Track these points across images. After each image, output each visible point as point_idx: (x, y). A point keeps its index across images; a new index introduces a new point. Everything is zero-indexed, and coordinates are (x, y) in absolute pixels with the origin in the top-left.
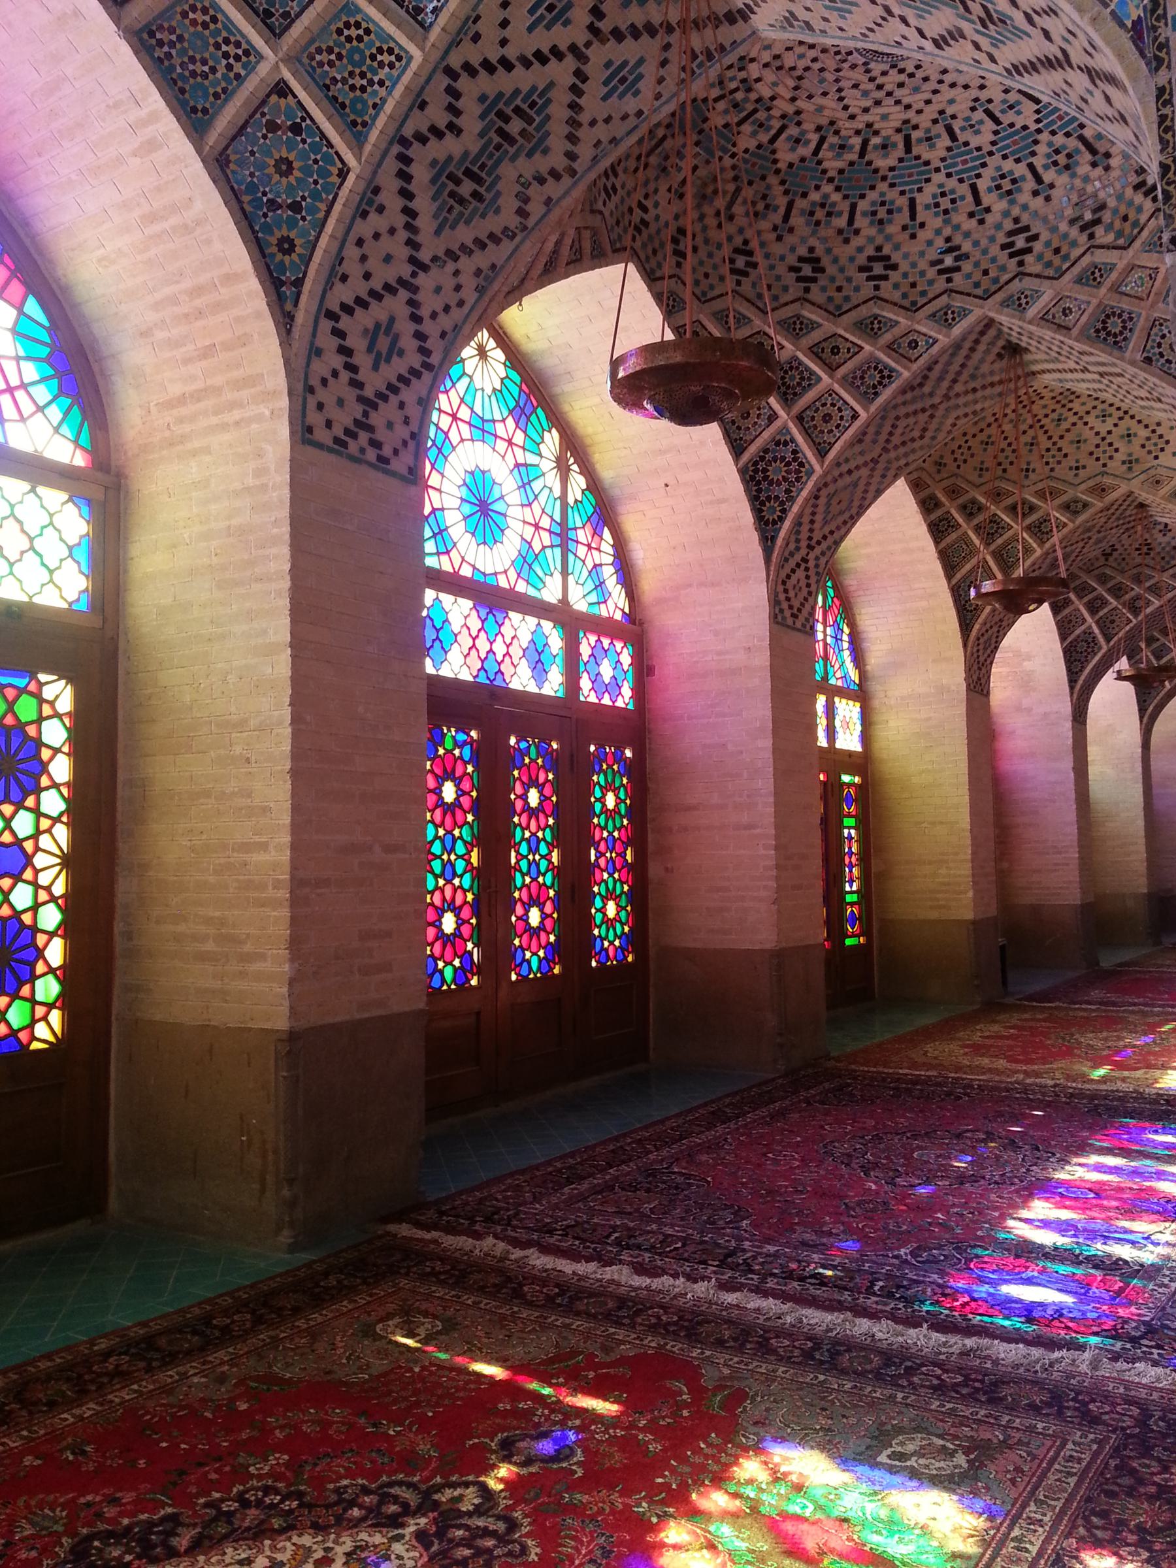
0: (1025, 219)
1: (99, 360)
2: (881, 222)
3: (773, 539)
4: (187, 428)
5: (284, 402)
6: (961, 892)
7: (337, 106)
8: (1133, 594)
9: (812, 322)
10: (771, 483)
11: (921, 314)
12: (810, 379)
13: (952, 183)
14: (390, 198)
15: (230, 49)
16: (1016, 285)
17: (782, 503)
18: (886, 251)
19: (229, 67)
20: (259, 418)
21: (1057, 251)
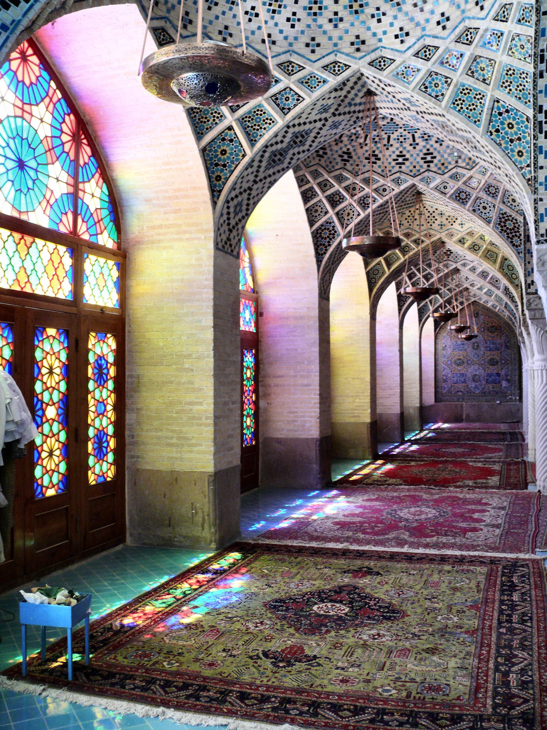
0: (431, 150)
1: (121, 207)
2: (376, 142)
3: (321, 261)
4: (162, 237)
5: (212, 234)
6: (364, 410)
7: (248, 134)
8: (427, 272)
9: (346, 177)
10: (322, 238)
11: (388, 179)
12: (343, 199)
13: (405, 133)
14: (256, 164)
15: (216, 115)
16: (426, 174)
17: (326, 247)
18: (376, 153)
19: (214, 120)
20: (199, 239)
21: (443, 164)
